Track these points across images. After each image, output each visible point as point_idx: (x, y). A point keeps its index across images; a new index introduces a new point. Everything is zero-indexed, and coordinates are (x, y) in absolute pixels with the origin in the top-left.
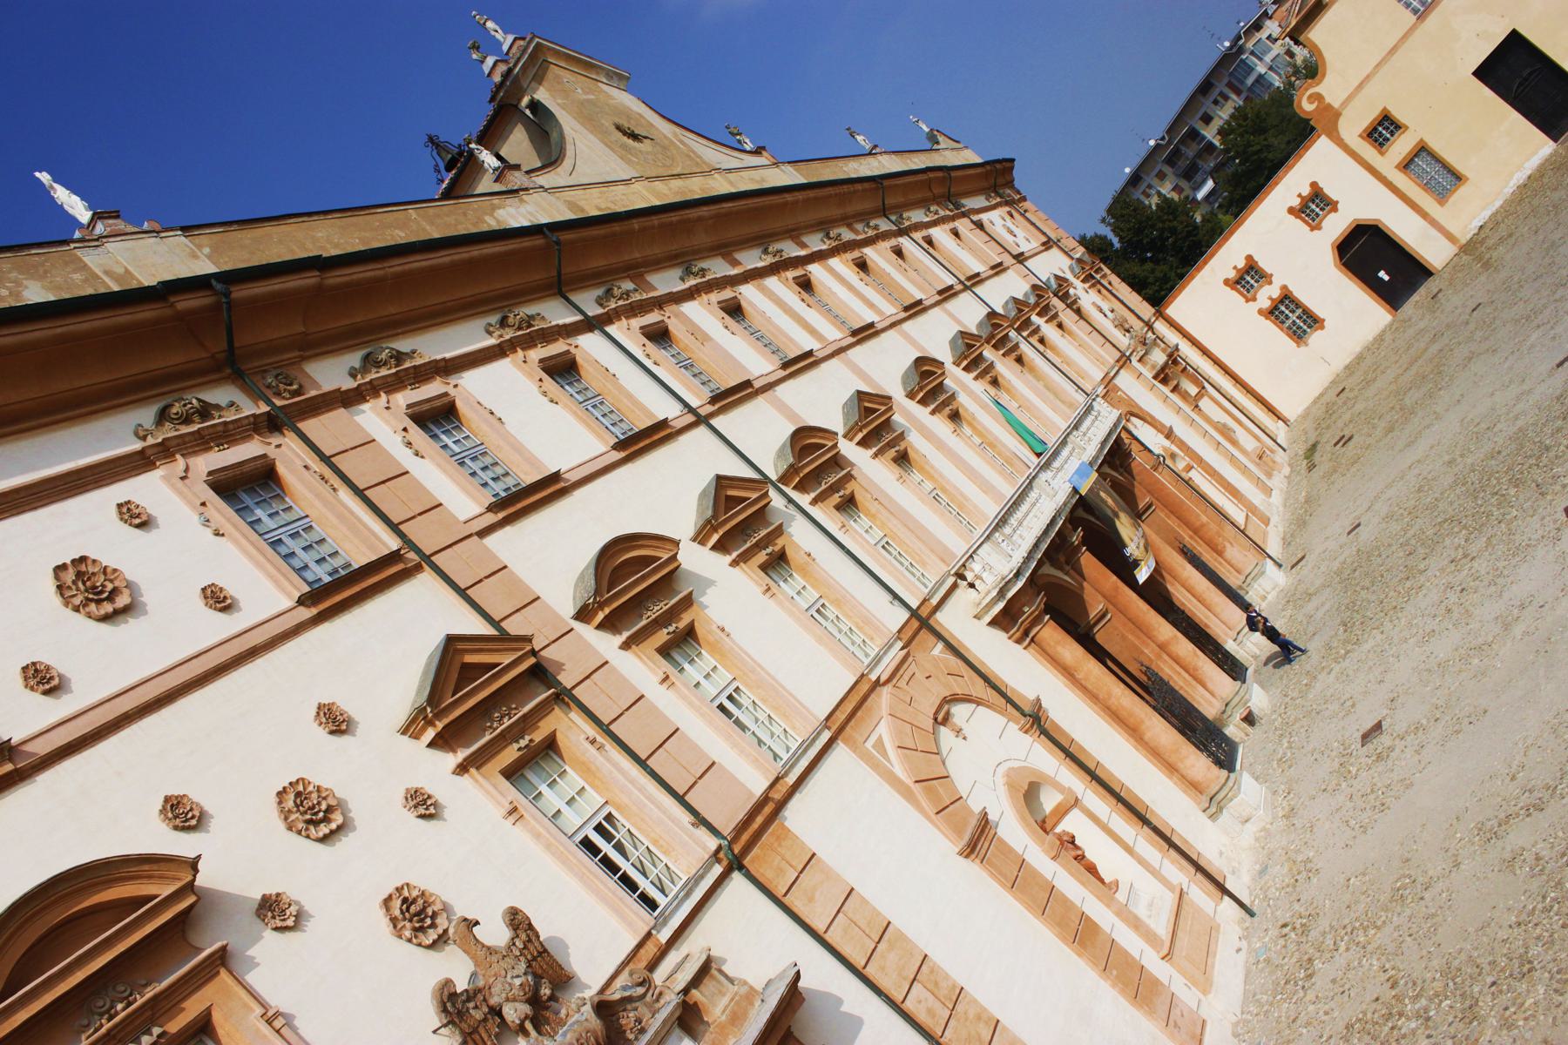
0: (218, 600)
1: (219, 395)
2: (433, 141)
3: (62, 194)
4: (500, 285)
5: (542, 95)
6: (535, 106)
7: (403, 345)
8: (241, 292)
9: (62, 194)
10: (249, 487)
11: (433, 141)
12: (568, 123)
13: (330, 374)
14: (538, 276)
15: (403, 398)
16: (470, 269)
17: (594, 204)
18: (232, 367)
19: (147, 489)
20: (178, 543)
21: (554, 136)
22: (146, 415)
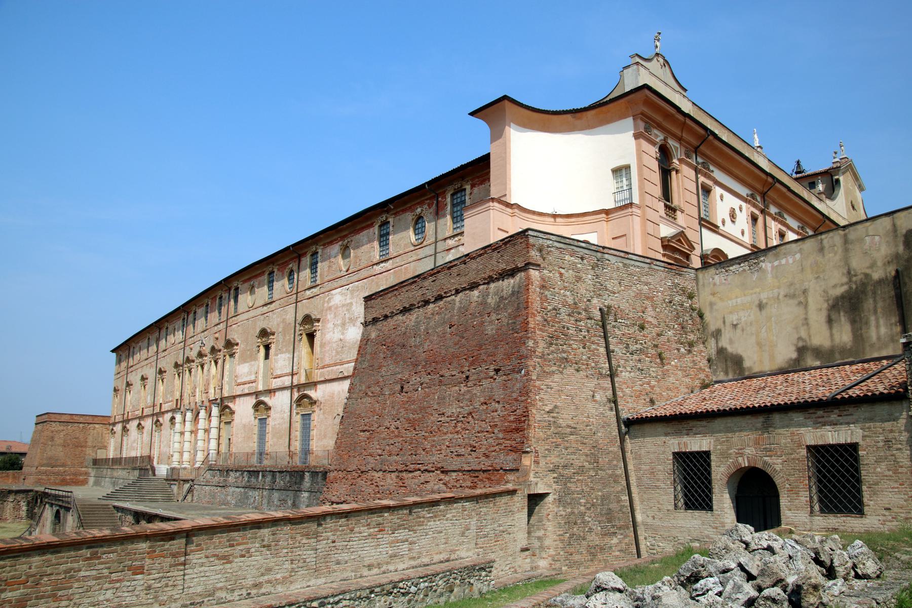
0: (743, 233)
1: (759, 199)
2: (798, 162)
3: (756, 136)
4: (807, 219)
5: (841, 179)
6: (838, 181)
7: (786, 216)
8: (777, 185)
9: (756, 136)
10: (754, 219)
11: (798, 162)
12: (841, 193)
13: (773, 210)
14: (814, 224)
15: (780, 226)
16: (806, 212)
17: (833, 217)
18: (764, 195)
19: (744, 205)
20: (743, 218)
21: (836, 192)
22: (749, 192)
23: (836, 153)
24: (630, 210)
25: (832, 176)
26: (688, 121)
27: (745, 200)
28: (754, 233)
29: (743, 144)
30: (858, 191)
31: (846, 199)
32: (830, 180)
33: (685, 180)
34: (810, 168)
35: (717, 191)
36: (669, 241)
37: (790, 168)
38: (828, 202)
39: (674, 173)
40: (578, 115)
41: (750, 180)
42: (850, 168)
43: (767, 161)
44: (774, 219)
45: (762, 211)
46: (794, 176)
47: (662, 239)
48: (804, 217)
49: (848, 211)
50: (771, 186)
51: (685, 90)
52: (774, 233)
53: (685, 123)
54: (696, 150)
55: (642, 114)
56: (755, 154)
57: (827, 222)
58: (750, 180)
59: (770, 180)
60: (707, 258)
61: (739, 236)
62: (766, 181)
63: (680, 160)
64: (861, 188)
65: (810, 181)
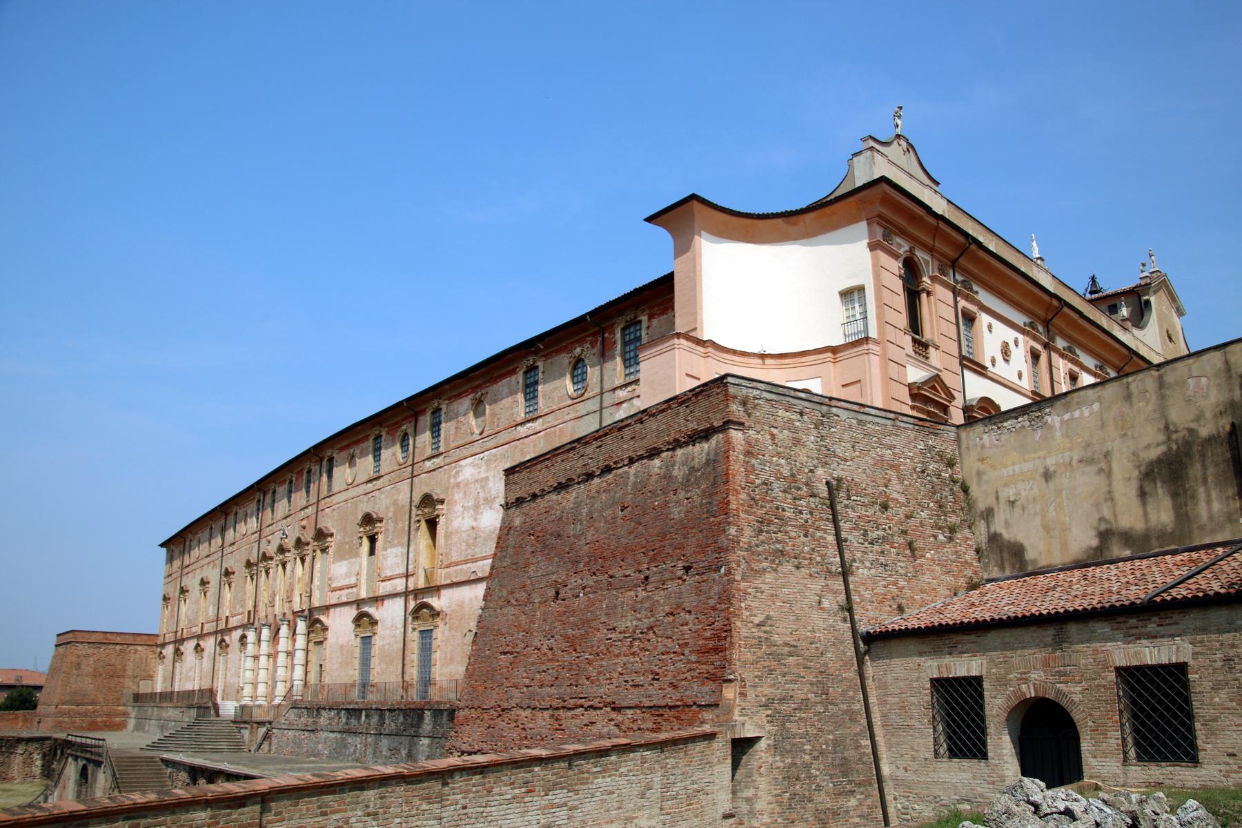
0: (1020, 376)
1: (1040, 328)
2: (1093, 278)
3: (1034, 243)
4: (1107, 356)
5: (1153, 299)
6: (1148, 303)
7: (1078, 352)
8: (1066, 309)
9: (1034, 243)
10: (1035, 356)
11: (1093, 278)
13: (1060, 343)
14: (1117, 362)
15: (1070, 365)
16: (1105, 345)
17: (1143, 351)
18: (1047, 324)
19: (1020, 337)
20: (1020, 356)
22: (1028, 320)
23: (1144, 265)
24: (865, 347)
25: (1140, 297)
26: (942, 225)
27: (1023, 331)
28: (1035, 375)
29: (1018, 255)
30: (1175, 316)
31: (1160, 327)
32: (1137, 301)
33: (939, 306)
34: (1110, 285)
35: (984, 319)
36: (919, 388)
37: (1082, 286)
38: (1135, 331)
39: (924, 296)
40: (793, 219)
41: (1027, 304)
42: (1165, 285)
43: (1050, 278)
44: (1063, 356)
45: (1046, 346)
46: (1088, 296)
47: (910, 386)
48: (1102, 352)
49: (1163, 343)
50: (1058, 312)
51: (937, 184)
52: (1062, 375)
53: (937, 228)
54: (954, 264)
55: (880, 216)
56: (1034, 268)
57: (1135, 358)
58: (1027, 304)
59: (1055, 303)
60: (973, 411)
61: (1015, 380)
62: (1050, 304)
63: (933, 278)
64: (1180, 312)
65: (1110, 303)
